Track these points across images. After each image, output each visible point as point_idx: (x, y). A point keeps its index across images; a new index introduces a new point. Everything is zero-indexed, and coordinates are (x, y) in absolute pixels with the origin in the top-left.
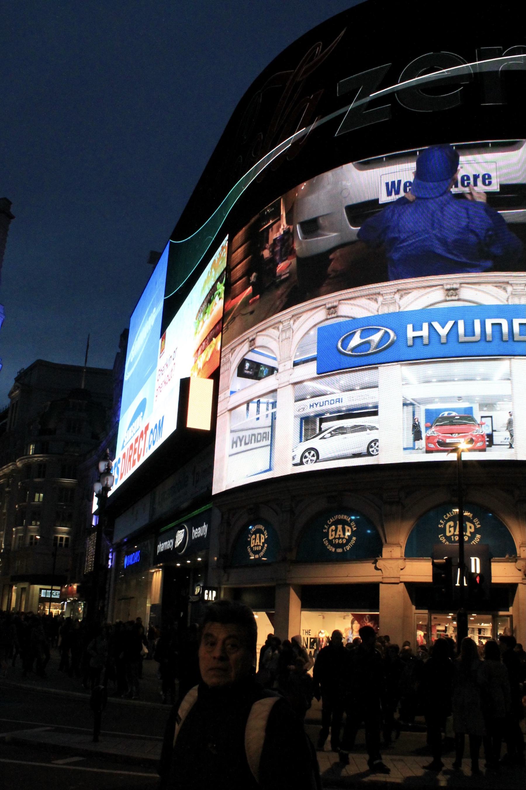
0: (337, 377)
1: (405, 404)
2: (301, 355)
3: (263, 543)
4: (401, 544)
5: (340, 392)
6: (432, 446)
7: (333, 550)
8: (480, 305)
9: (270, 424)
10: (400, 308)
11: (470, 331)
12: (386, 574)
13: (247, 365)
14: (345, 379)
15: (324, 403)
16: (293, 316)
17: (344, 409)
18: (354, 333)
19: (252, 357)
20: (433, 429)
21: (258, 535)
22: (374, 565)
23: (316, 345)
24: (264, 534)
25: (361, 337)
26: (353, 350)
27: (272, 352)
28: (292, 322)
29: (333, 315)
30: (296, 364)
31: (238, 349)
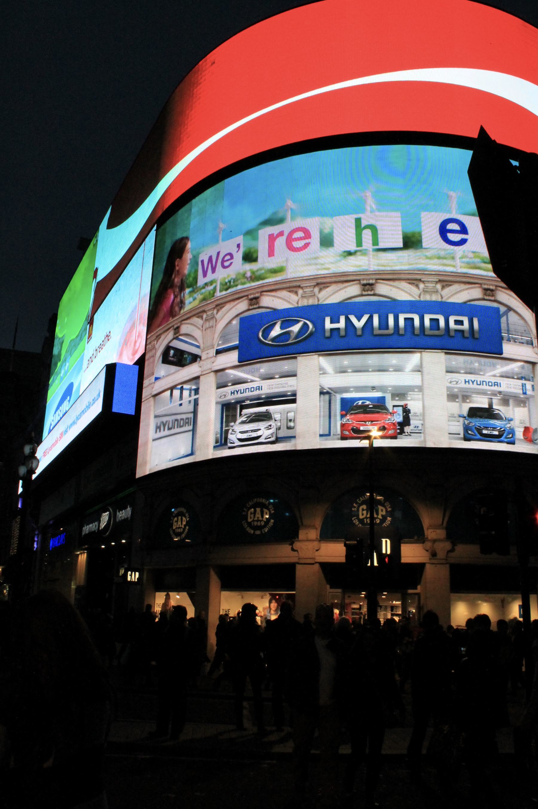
0: (258, 365)
1: (322, 393)
2: (223, 343)
3: (185, 526)
4: (317, 526)
6: (347, 433)
7: (252, 532)
8: (394, 301)
9: (192, 410)
10: (318, 301)
11: (384, 324)
12: (302, 554)
13: (172, 352)
14: (264, 368)
15: (245, 391)
16: (217, 306)
17: (263, 396)
18: (275, 324)
19: (176, 344)
20: (348, 417)
21: (180, 517)
22: (291, 546)
23: (238, 334)
24: (185, 517)
25: (282, 328)
27: (196, 339)
28: (215, 311)
29: (255, 306)
30: (218, 352)
31: (163, 337)
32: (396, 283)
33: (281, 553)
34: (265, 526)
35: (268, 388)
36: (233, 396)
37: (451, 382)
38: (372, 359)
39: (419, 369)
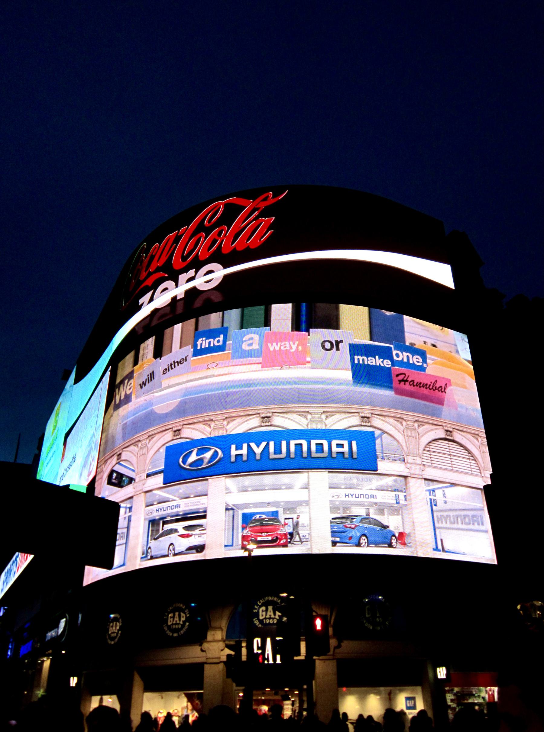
1: (227, 509)
2: (152, 468)
3: (118, 630)
4: (223, 628)
5: (180, 499)
7: (171, 634)
9: (126, 526)
10: (227, 432)
11: (278, 450)
12: (210, 655)
13: (115, 475)
16: (149, 436)
17: (181, 513)
18: (192, 451)
19: (118, 468)
21: (115, 623)
22: (200, 647)
24: (119, 622)
25: (197, 455)
26: (190, 465)
27: (132, 465)
28: (148, 440)
29: (178, 437)
30: (148, 476)
31: (109, 461)
32: (289, 416)
33: (192, 654)
34: (181, 629)
35: (185, 506)
36: (157, 514)
37: (333, 497)
38: (269, 479)
39: (306, 487)
